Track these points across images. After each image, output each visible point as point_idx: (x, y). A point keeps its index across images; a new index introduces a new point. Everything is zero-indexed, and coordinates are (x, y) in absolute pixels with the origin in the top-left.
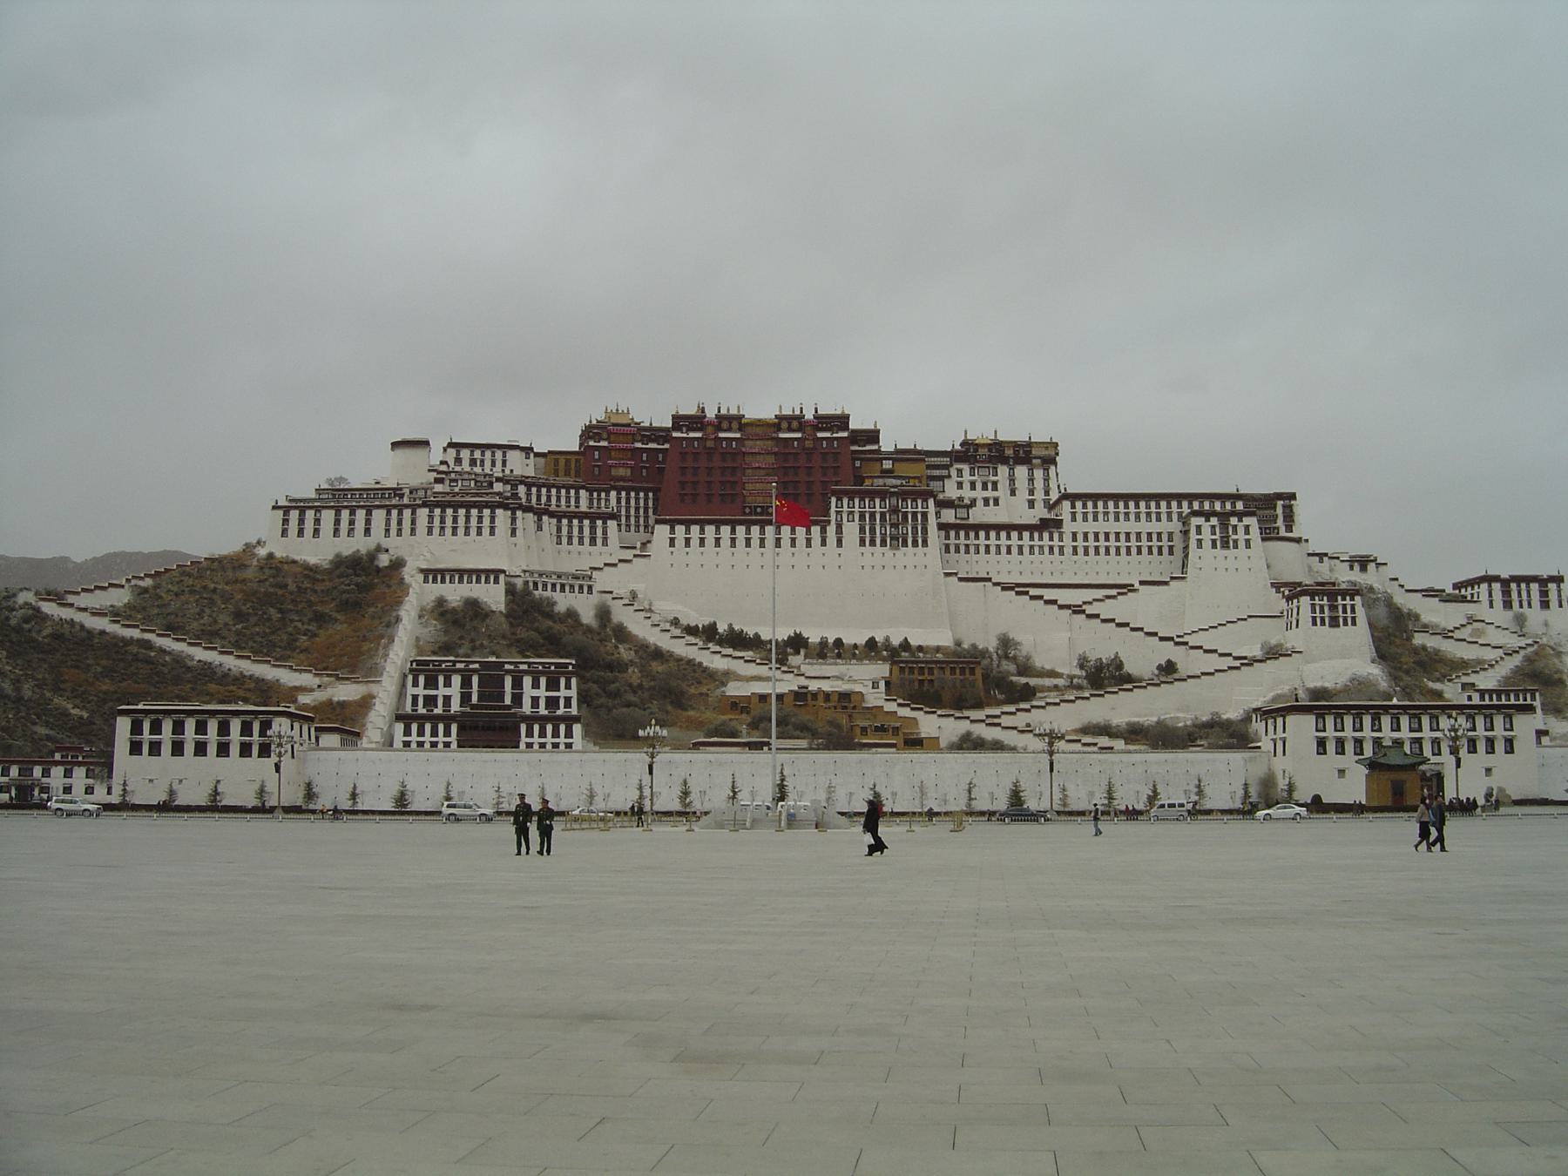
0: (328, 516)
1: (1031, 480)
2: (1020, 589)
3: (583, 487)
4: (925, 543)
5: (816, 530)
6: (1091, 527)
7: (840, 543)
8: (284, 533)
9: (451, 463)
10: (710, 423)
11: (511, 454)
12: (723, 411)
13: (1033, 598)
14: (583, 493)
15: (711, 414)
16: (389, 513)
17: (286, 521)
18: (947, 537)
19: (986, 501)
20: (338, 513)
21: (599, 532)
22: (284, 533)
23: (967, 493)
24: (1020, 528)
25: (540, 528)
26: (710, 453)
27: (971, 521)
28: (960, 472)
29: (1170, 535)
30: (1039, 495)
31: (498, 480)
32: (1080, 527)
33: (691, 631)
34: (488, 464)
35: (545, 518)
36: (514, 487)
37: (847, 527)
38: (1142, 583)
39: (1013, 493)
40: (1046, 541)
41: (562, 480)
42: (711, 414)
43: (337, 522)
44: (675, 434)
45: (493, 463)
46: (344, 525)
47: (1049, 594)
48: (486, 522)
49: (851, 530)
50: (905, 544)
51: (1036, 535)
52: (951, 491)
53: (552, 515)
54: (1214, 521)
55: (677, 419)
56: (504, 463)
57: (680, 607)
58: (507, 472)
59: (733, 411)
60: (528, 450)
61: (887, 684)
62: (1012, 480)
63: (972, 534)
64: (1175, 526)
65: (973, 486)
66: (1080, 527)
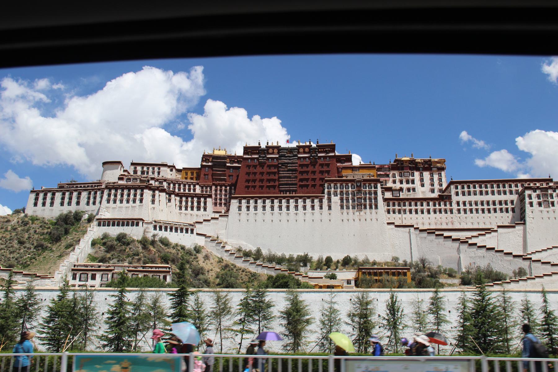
0: (58, 195)
1: (432, 180)
2: (430, 232)
3: (198, 184)
4: (376, 207)
5: (316, 201)
6: (467, 198)
7: (330, 208)
8: (36, 204)
9: (132, 173)
10: (263, 150)
11: (162, 168)
12: (270, 144)
13: (437, 235)
14: (197, 187)
15: (263, 146)
16: (90, 193)
17: (37, 199)
18: (388, 206)
19: (409, 190)
20: (64, 194)
21: (202, 204)
22: (36, 204)
23: (398, 186)
24: (428, 200)
25: (170, 200)
26: (262, 165)
27: (401, 197)
28: (394, 176)
29: (512, 202)
30: (436, 187)
31: (153, 179)
32: (461, 198)
33: (247, 254)
34: (150, 173)
35: (173, 196)
36: (161, 183)
37: (333, 198)
38: (499, 227)
39: (423, 185)
40: (443, 207)
41: (189, 180)
42: (263, 146)
43: (63, 199)
44: (245, 156)
45: (153, 173)
46: (66, 200)
47: (446, 234)
48: (138, 197)
49: (336, 200)
50: (365, 208)
51: (437, 203)
52: (390, 184)
53: (177, 195)
54: (538, 192)
55: (247, 150)
56: (159, 173)
57: (244, 243)
58: (160, 176)
59: (275, 144)
60: (172, 167)
61: (356, 281)
62: (422, 180)
63: (402, 204)
64: (515, 197)
65: (401, 182)
66: (461, 198)
